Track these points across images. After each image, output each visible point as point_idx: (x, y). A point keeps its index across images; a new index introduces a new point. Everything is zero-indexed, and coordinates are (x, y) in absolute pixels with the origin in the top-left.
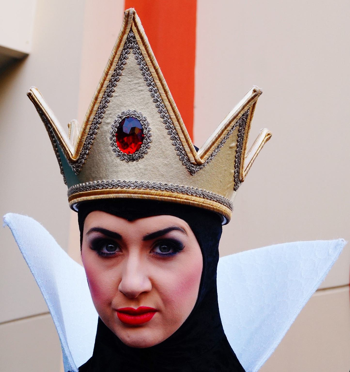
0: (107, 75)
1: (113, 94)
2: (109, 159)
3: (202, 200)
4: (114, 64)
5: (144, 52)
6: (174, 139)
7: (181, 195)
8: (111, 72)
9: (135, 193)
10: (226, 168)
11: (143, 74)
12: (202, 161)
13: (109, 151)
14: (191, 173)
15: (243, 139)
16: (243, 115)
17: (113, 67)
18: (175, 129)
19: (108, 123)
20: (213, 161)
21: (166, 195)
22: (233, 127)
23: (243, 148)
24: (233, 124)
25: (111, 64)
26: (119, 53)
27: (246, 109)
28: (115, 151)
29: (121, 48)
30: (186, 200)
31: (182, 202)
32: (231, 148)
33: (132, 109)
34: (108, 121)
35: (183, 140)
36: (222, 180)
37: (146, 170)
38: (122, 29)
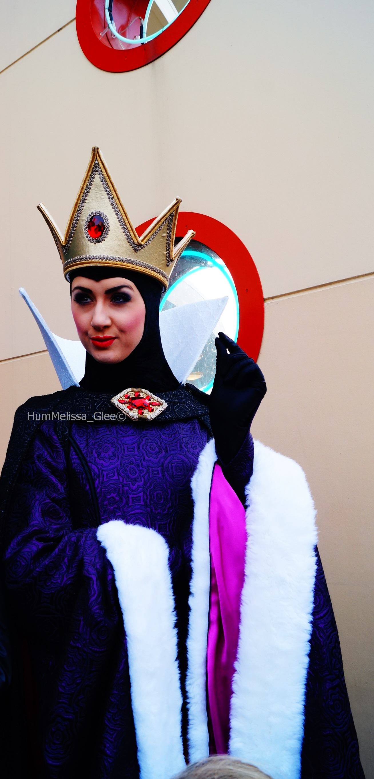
0: (82, 189)
1: (86, 201)
2: (84, 243)
3: (143, 269)
4: (87, 182)
5: (105, 174)
6: (123, 228)
7: (129, 265)
8: (85, 187)
9: (99, 263)
10: (160, 250)
11: (104, 187)
12: (143, 243)
13: (84, 238)
14: (136, 250)
16: (170, 215)
17: (86, 184)
19: (83, 220)
21: (119, 264)
24: (163, 220)
25: (85, 182)
26: (89, 174)
27: (172, 210)
28: (87, 237)
29: (91, 171)
32: (163, 237)
33: (98, 210)
34: (84, 218)
35: (130, 229)
37: (106, 248)
38: (91, 159)
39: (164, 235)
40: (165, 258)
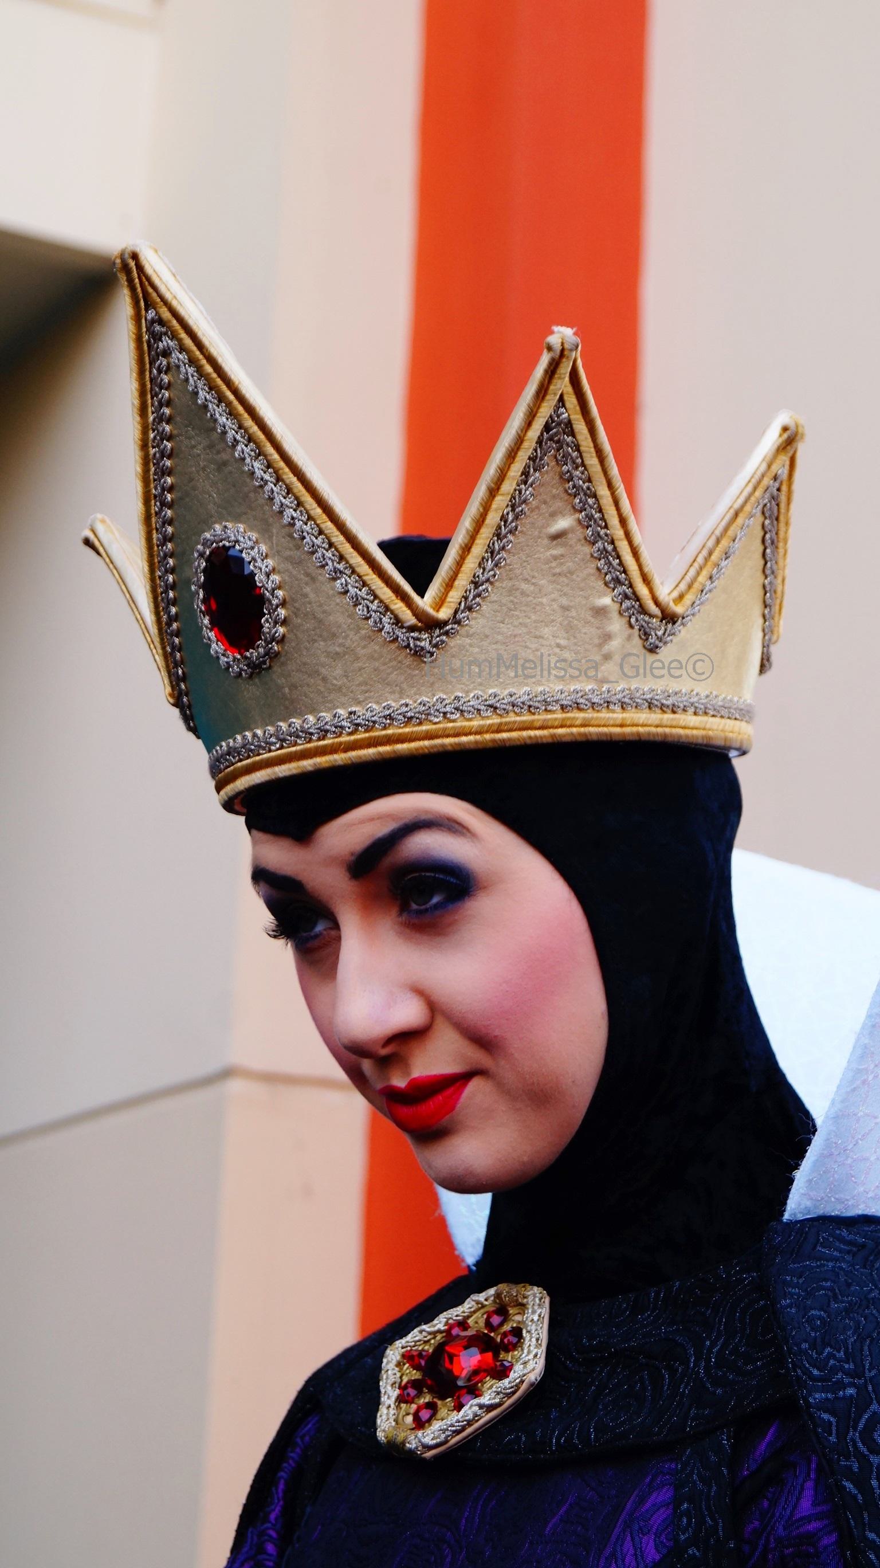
10: (564, 601)
12: (444, 614)
15: (595, 496)
16: (547, 428)
18: (331, 545)
20: (493, 597)
22: (526, 474)
23: (614, 521)
30: (426, 743)
31: (417, 749)
35: (364, 568)
36: (563, 642)
39: (564, 523)
40: (617, 625)
